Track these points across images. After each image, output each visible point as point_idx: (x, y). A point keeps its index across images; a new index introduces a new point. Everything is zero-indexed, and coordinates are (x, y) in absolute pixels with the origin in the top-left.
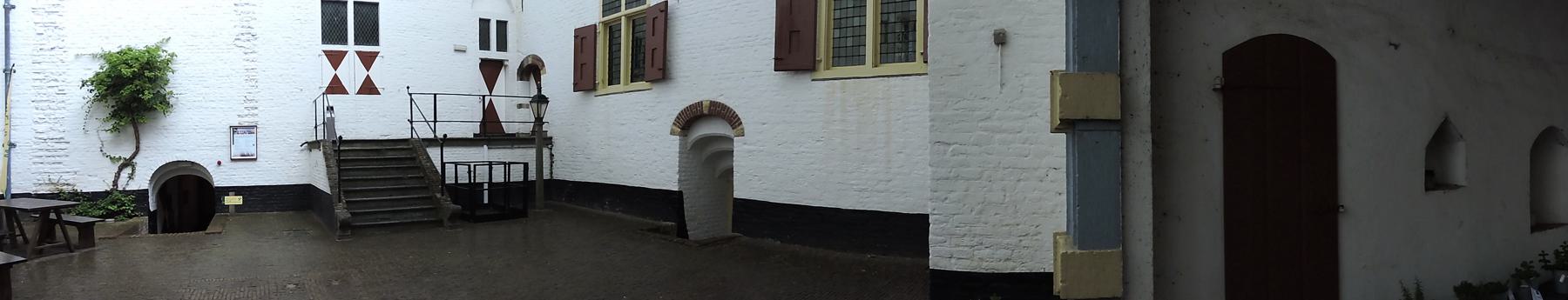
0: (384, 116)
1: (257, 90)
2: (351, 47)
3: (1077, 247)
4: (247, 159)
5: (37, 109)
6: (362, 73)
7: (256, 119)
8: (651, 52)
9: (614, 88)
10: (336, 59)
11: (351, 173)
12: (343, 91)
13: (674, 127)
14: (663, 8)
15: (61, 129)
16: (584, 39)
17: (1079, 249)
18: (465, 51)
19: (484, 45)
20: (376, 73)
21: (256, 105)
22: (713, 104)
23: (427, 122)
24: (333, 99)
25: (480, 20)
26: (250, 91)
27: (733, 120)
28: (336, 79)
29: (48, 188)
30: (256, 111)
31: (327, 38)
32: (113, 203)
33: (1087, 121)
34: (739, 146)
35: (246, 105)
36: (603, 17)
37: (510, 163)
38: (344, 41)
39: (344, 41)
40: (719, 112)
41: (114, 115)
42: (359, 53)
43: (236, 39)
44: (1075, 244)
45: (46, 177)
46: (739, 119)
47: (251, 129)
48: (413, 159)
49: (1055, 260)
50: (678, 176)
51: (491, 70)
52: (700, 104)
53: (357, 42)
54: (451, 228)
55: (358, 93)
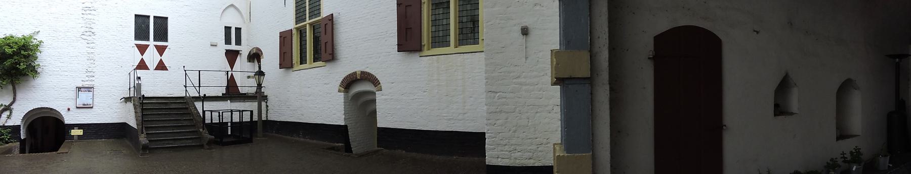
0: (170, 83)
1: (94, 66)
2: (151, 43)
3: (565, 152)
6: (157, 58)
7: (93, 83)
9: (303, 66)
10: (142, 49)
11: (150, 116)
12: (146, 68)
13: (340, 88)
14: (330, 18)
16: (285, 38)
17: (567, 153)
18: (216, 46)
19: (228, 41)
20: (165, 58)
21: (93, 74)
22: (363, 73)
23: (195, 87)
24: (140, 73)
25: (225, 27)
26: (90, 66)
27: (375, 81)
28: (142, 60)
30: (93, 78)
31: (137, 37)
33: (571, 78)
34: (379, 97)
35: (87, 74)
36: (296, 25)
37: (243, 111)
38: (148, 39)
39: (148, 39)
40: (367, 77)
44: (565, 150)
46: (378, 81)
47: (89, 89)
48: (186, 108)
49: (554, 159)
50: (344, 116)
51: (232, 56)
52: (355, 73)
53: (154, 41)
54: (208, 149)
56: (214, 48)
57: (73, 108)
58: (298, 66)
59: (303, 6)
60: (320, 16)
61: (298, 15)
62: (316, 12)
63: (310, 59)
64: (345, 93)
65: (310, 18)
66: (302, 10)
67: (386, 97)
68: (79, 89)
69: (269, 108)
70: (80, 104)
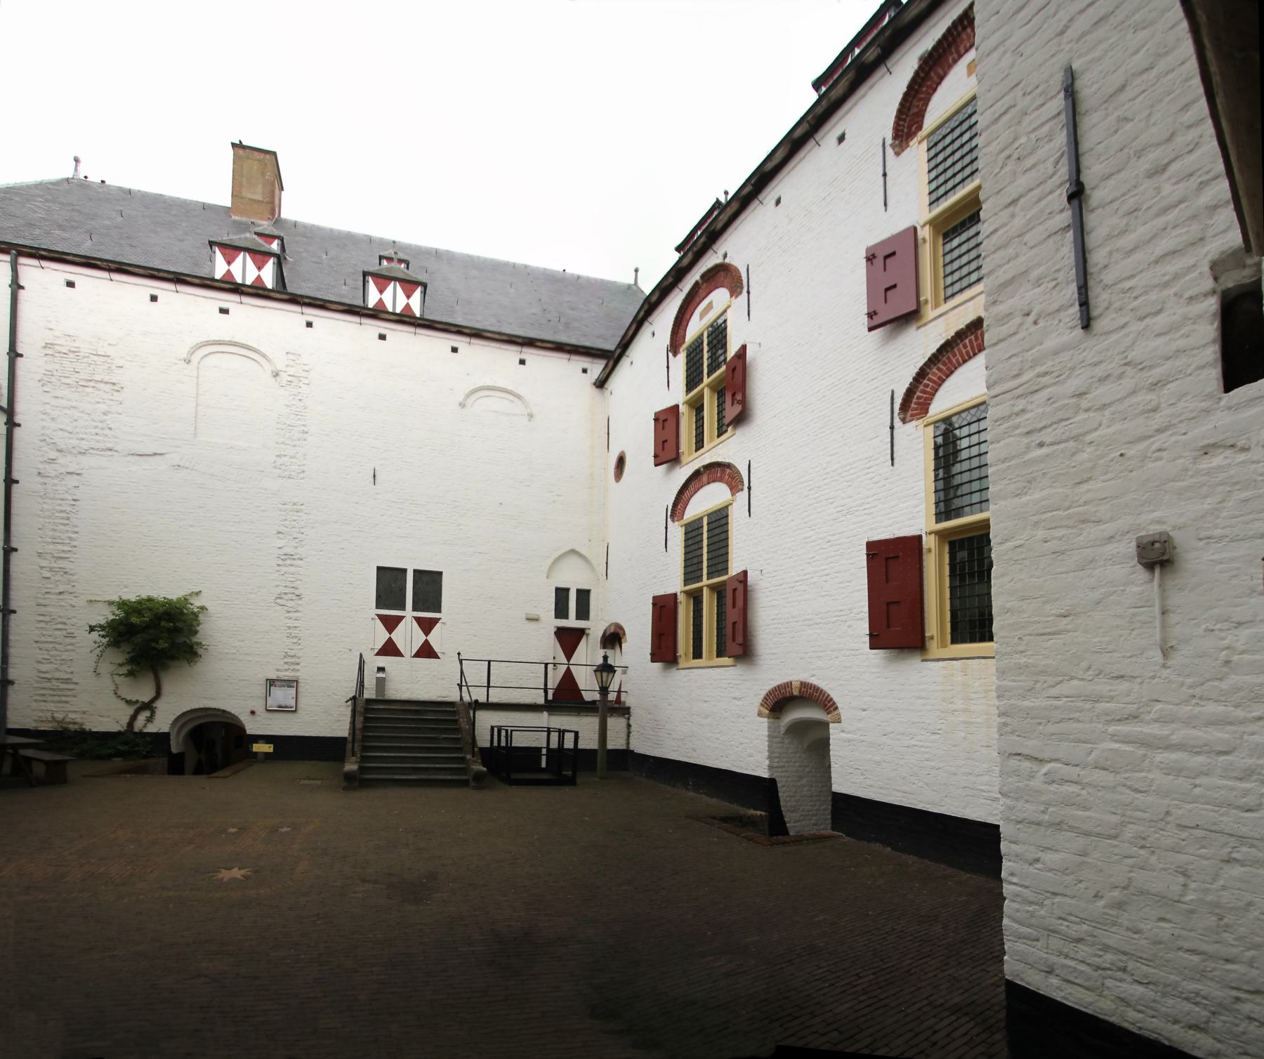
0: (442, 679)
1: (300, 647)
2: (409, 613)
4: (282, 710)
5: (41, 649)
6: (419, 638)
7: (297, 674)
8: (731, 625)
9: (697, 662)
10: (391, 624)
12: (397, 653)
14: (742, 579)
15: (69, 670)
16: (664, 609)
18: (537, 620)
19: (561, 611)
20: (435, 638)
21: (298, 660)
24: (384, 661)
25: (557, 590)
26: (293, 647)
27: (828, 704)
29: (51, 725)
30: (297, 667)
31: (380, 603)
32: (126, 743)
34: (835, 732)
35: (286, 660)
36: (685, 585)
38: (403, 608)
40: (810, 695)
41: (131, 661)
42: (418, 620)
43: (277, 598)
45: (49, 715)
46: (834, 703)
47: (292, 683)
50: (767, 762)
51: (569, 639)
53: (414, 610)
55: (415, 656)
56: (533, 625)
57: (259, 708)
58: (687, 660)
59: (698, 553)
60: (727, 574)
61: (690, 569)
62: (720, 567)
63: (710, 652)
64: (772, 720)
65: (710, 576)
66: (695, 561)
67: (849, 736)
68: (271, 683)
69: (632, 729)
70: (272, 703)
